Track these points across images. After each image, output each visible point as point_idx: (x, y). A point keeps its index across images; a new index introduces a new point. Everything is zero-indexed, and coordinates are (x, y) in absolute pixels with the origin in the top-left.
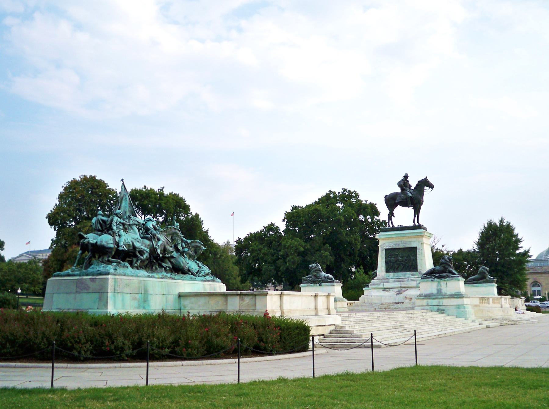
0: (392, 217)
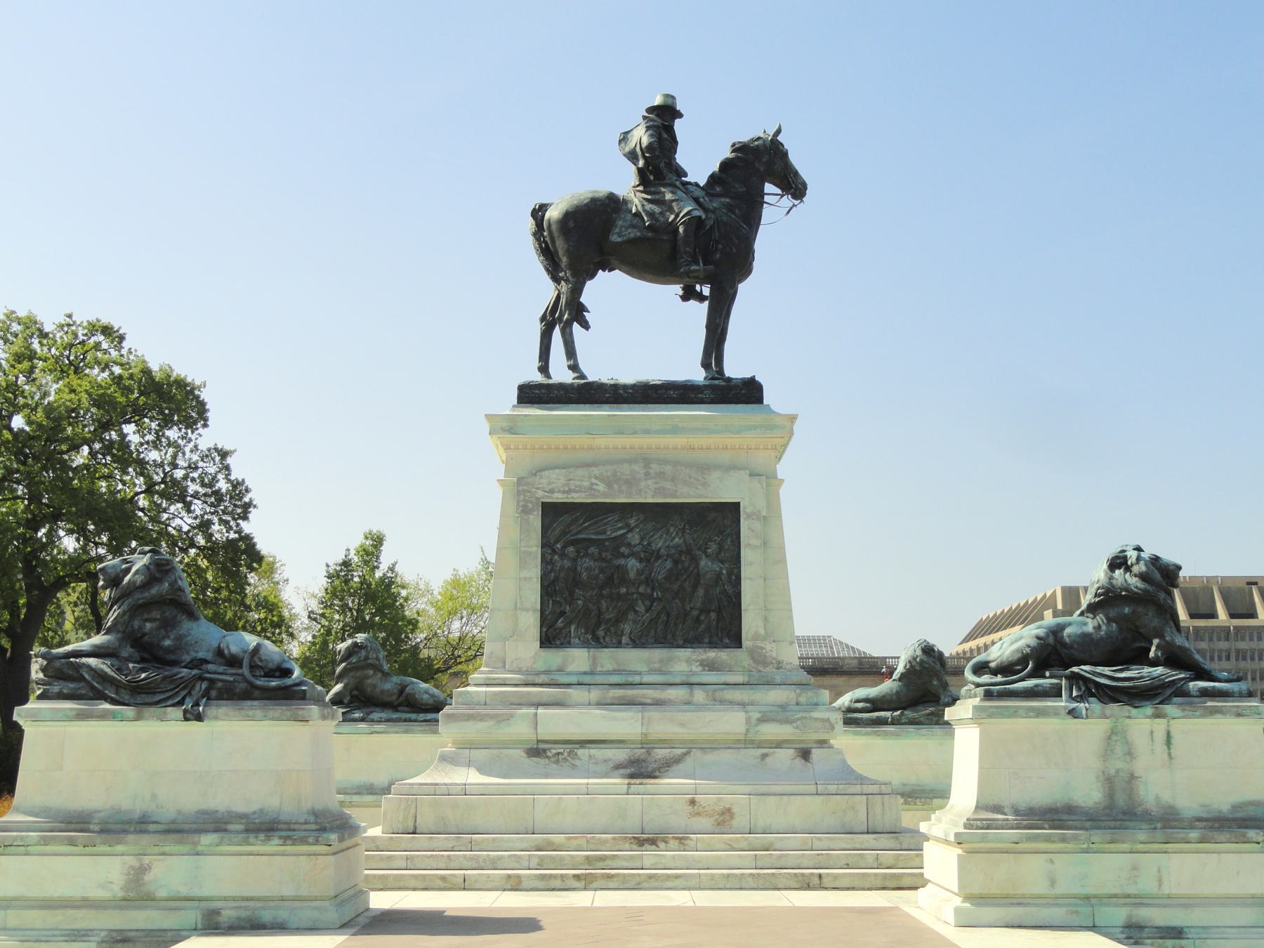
0: (576, 327)
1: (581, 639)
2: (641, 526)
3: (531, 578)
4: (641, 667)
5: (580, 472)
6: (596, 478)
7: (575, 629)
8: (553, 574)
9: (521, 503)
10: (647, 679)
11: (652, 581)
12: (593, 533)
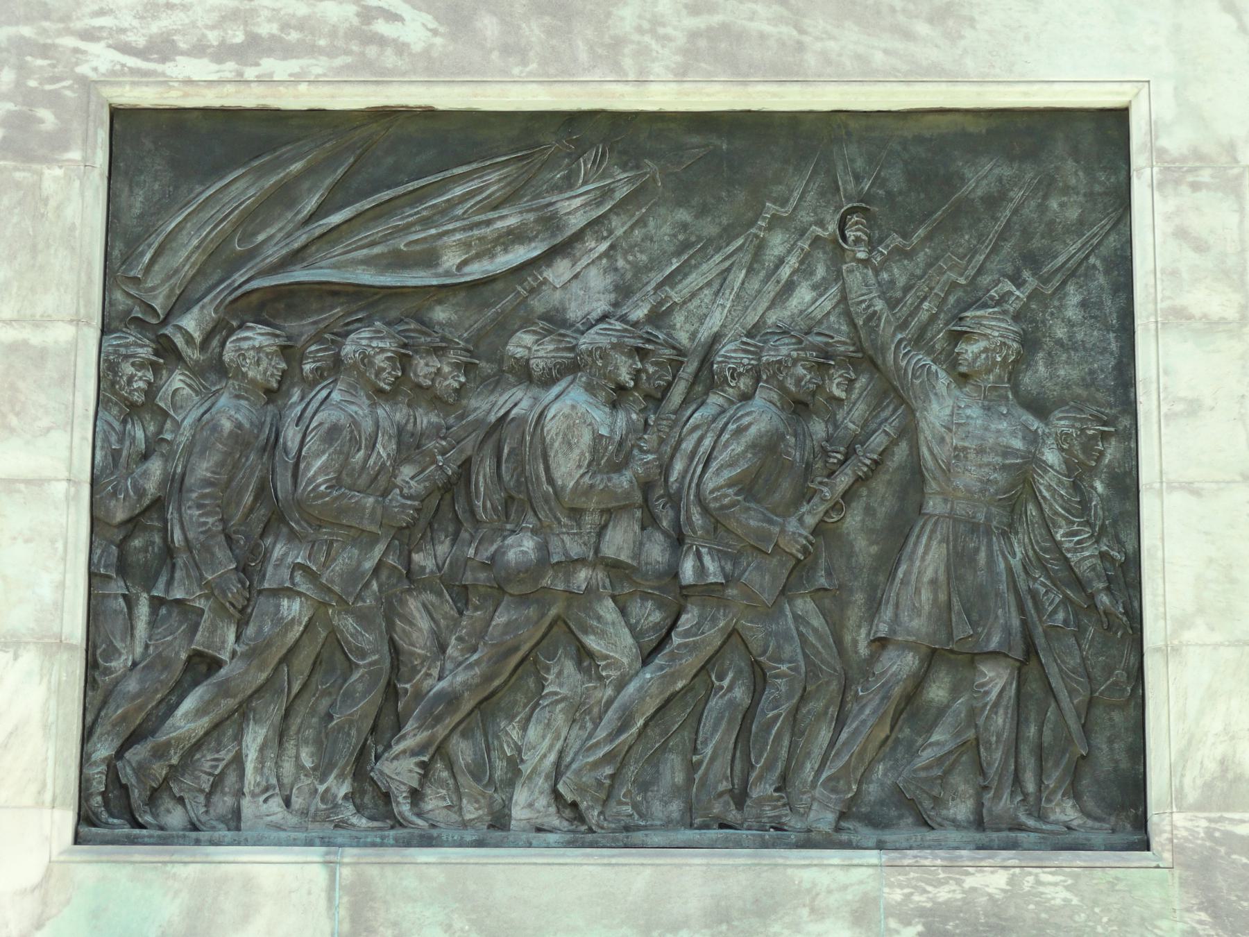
1: (297, 802)
2: (619, 226)
7: (262, 749)
8: (155, 467)
11: (674, 500)
12: (367, 262)
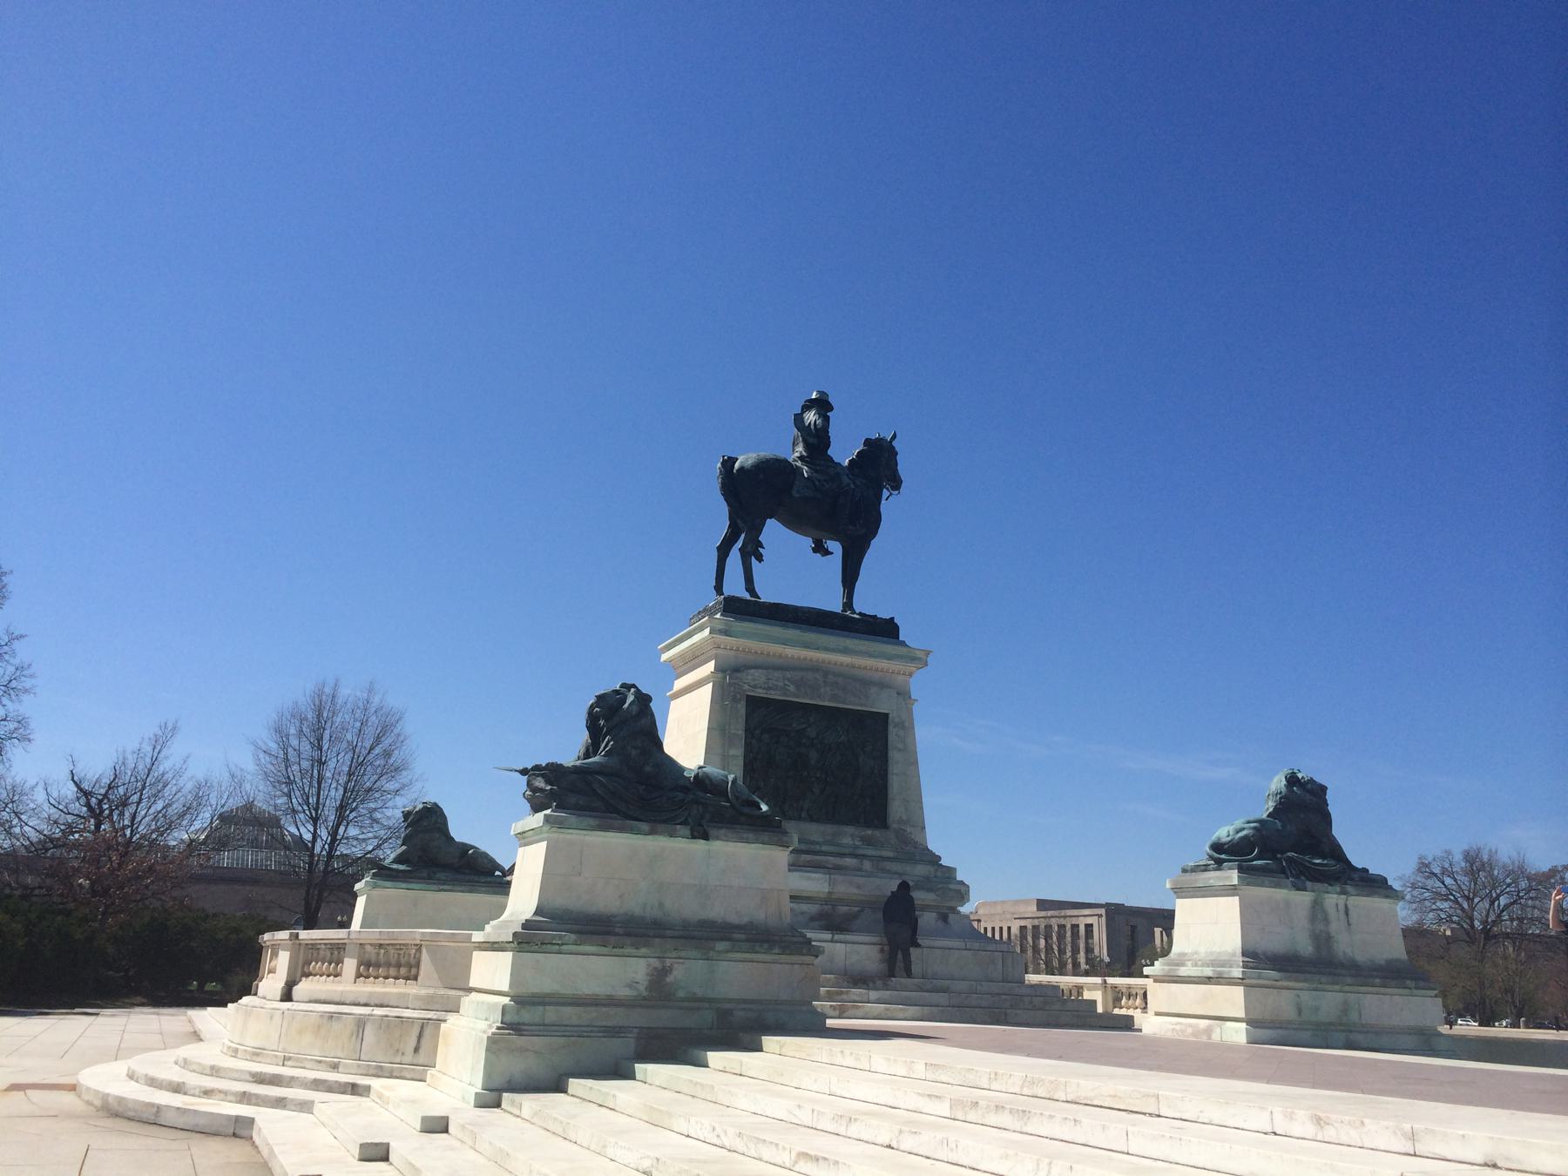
3: (737, 756)
4: (815, 837)
5: (777, 674)
6: (788, 680)
9: (732, 694)
10: (824, 848)
